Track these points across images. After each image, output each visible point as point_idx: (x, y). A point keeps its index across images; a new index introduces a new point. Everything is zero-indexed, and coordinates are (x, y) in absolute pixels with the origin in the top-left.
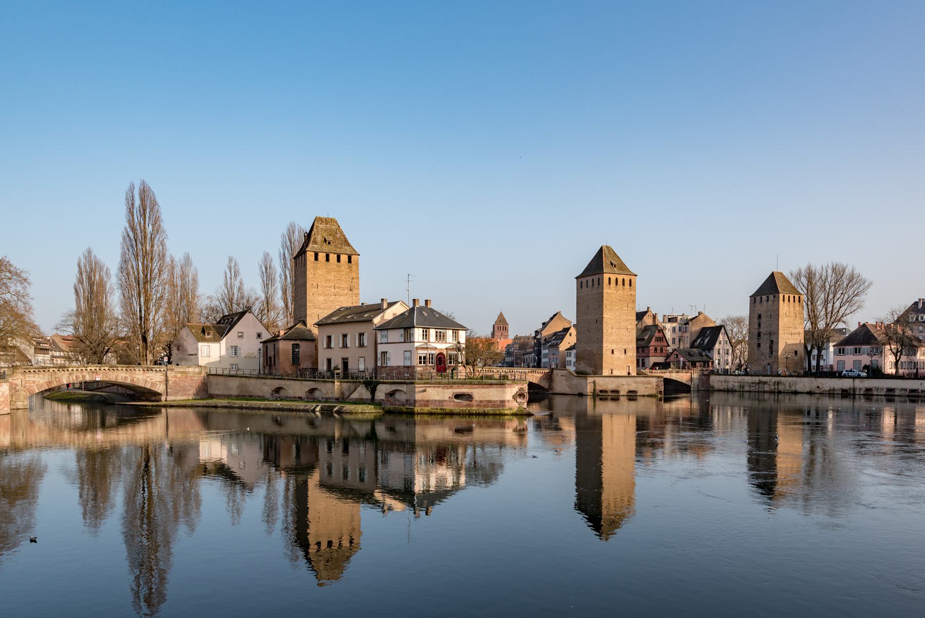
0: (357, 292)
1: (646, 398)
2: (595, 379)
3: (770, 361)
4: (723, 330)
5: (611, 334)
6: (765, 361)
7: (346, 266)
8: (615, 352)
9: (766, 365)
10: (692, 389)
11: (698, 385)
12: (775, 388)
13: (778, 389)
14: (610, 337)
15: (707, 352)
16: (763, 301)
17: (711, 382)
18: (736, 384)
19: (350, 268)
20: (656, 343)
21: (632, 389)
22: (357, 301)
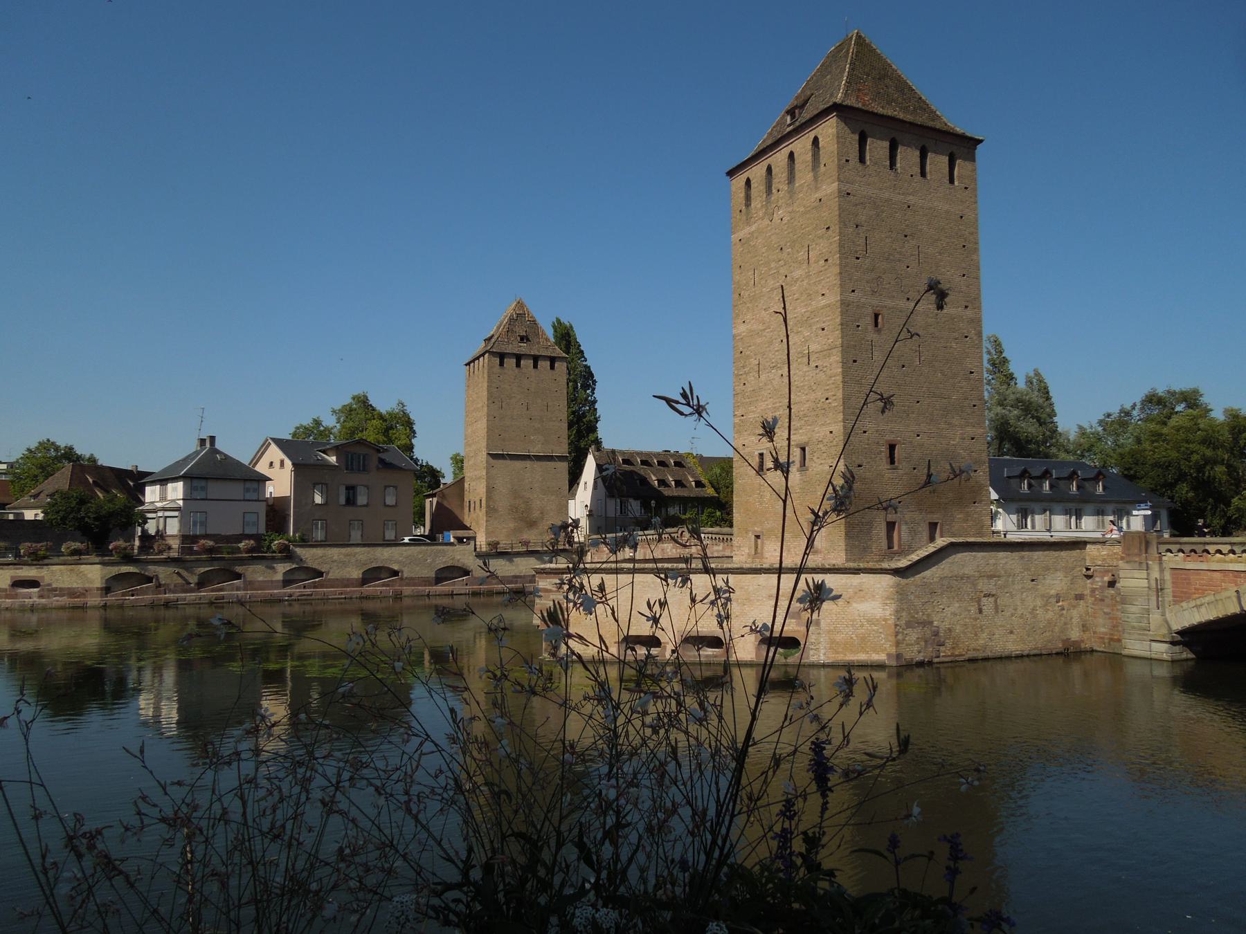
14: (753, 408)
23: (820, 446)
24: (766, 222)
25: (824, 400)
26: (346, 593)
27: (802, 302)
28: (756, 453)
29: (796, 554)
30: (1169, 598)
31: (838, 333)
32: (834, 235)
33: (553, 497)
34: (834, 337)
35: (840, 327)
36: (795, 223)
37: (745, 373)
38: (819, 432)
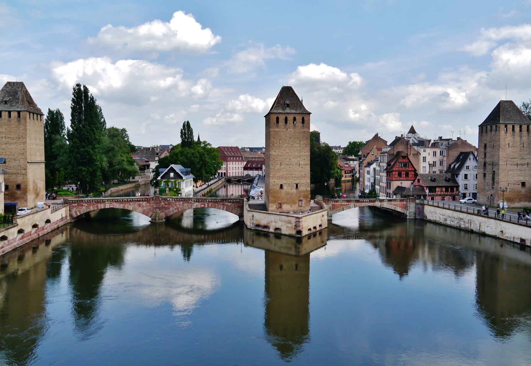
0: (25, 140)
1: (287, 237)
3: (492, 192)
4: (471, 157)
7: (16, 120)
9: (490, 196)
10: (408, 217)
11: (415, 213)
12: (469, 226)
15: (455, 177)
16: (488, 131)
17: (425, 212)
19: (19, 121)
20: (400, 168)
22: (24, 148)
24: (285, 130)
26: (29, 239)
30: (331, 209)
31: (309, 161)
33: (42, 182)
34: (309, 162)
36: (296, 134)
37: (275, 164)
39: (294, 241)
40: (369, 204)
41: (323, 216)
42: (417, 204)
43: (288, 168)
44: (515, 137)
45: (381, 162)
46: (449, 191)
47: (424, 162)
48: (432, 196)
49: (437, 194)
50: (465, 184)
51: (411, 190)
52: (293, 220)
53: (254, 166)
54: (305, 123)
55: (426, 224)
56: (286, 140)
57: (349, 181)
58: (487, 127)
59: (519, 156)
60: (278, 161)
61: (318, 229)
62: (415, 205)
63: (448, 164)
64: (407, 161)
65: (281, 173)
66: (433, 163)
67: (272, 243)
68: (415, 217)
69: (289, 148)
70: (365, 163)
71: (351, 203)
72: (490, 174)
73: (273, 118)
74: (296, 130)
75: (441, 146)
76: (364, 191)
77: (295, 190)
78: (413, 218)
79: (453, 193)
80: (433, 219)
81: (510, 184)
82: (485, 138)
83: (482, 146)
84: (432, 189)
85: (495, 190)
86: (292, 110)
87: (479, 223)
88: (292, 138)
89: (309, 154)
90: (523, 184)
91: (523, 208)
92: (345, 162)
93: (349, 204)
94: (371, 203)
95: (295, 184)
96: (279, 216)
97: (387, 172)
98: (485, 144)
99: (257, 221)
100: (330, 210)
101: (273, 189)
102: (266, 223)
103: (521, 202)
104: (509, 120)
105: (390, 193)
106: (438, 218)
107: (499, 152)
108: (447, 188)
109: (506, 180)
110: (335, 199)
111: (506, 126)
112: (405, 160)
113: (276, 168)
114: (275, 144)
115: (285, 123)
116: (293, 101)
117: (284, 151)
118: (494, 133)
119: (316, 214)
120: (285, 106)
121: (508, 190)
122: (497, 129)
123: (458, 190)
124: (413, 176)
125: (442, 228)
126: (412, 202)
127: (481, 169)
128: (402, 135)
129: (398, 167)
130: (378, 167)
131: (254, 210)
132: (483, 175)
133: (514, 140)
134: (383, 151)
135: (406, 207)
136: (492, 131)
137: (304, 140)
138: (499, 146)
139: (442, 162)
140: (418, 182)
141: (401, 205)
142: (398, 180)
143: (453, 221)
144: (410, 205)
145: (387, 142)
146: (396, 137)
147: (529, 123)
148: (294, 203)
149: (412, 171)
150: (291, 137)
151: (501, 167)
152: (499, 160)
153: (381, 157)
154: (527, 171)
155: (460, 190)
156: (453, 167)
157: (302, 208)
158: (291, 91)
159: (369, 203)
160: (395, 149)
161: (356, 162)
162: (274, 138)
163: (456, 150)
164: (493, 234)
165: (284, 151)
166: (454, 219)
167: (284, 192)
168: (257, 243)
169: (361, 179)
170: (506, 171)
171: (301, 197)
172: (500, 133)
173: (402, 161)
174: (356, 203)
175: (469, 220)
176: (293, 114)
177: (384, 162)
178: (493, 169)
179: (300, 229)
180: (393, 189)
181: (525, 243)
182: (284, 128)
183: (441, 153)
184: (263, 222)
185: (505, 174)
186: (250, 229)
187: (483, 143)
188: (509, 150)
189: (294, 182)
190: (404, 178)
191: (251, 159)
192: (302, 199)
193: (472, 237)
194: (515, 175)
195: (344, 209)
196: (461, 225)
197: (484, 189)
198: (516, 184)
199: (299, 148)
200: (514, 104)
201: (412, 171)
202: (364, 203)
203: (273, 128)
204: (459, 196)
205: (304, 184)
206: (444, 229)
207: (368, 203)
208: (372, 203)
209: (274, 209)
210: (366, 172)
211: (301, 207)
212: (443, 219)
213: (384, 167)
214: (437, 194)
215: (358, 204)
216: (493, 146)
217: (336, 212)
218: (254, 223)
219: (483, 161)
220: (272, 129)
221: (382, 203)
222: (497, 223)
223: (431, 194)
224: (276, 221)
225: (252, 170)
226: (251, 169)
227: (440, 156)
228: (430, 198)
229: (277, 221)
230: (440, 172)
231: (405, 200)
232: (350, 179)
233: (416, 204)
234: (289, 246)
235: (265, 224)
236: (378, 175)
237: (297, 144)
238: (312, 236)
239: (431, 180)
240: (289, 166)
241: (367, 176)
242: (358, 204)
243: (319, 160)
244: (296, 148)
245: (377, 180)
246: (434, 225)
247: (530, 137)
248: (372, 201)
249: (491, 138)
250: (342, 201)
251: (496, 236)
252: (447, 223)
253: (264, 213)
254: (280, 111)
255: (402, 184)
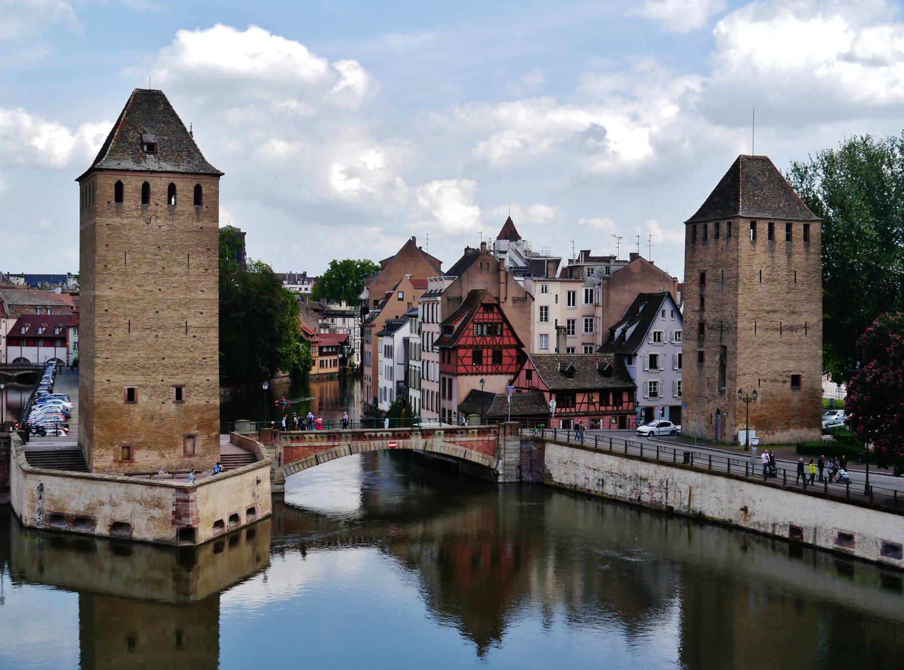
1: (148, 550)
2: (43, 479)
3: (721, 403)
4: (667, 307)
5: (124, 345)
6: (711, 403)
8: (142, 398)
9: (714, 412)
10: (501, 479)
11: (519, 467)
12: (662, 497)
13: (666, 503)
14: (121, 355)
15: (626, 362)
18: (591, 475)
20: (478, 339)
21: (122, 513)
23: (198, 388)
24: (141, 222)
25: (201, 359)
27: (181, 291)
28: (126, 387)
29: (171, 458)
30: (282, 461)
31: (216, 319)
32: (214, 255)
34: (215, 321)
35: (218, 316)
36: (174, 235)
37: (111, 327)
38: (196, 379)
39: (170, 559)
40: (391, 443)
41: (258, 482)
42: (524, 441)
43: (151, 339)
44: (776, 255)
45: (424, 322)
46: (611, 403)
47: (544, 322)
48: (564, 418)
49: (577, 411)
50: (651, 383)
51: (509, 401)
52: (169, 497)
53: (40, 332)
54: (204, 201)
55: (550, 495)
56: (144, 253)
57: (330, 377)
58: (706, 226)
59: (786, 306)
60: (121, 317)
61: (244, 520)
62: (518, 443)
63: (607, 326)
64: (498, 319)
65: (132, 354)
66: (566, 325)
67: (101, 569)
68: (520, 477)
69: (153, 278)
70: (379, 323)
71: (341, 443)
72: (716, 354)
73: (106, 184)
74: (175, 223)
75: (589, 278)
76: (377, 406)
77: (173, 406)
78: (515, 480)
79: (620, 408)
80: (568, 483)
81: (764, 381)
82: (702, 257)
83: (693, 278)
84: (565, 397)
85: (727, 398)
86: (162, 164)
87: (687, 488)
88: (164, 246)
89: (214, 295)
90: (796, 381)
91: (795, 445)
92: (320, 321)
93: (334, 446)
94: (397, 441)
95: (173, 386)
96: (124, 485)
97: (442, 352)
98: (701, 273)
99: (54, 502)
100: (277, 462)
101: (104, 403)
102: (82, 509)
103: (789, 427)
104: (759, 209)
105: (450, 412)
106: (584, 476)
107: (736, 295)
108: (604, 394)
109: (753, 369)
110: (292, 432)
111: (753, 226)
112: (491, 316)
113: (115, 339)
114: (110, 266)
115: (143, 202)
116: (168, 135)
117: (138, 285)
118: (724, 243)
119: (238, 478)
120: (143, 150)
121: (759, 398)
122: (730, 231)
123: (632, 398)
124: (515, 362)
125: (592, 505)
126: (511, 434)
127: (692, 342)
128: (483, 244)
129: (473, 335)
130: (417, 336)
131: (44, 471)
132: (696, 355)
133: (773, 261)
134: (430, 289)
135: (494, 450)
136: (718, 238)
137: (203, 253)
138: (737, 277)
139: (591, 320)
140: (527, 379)
141: (480, 444)
142: (472, 374)
143: (620, 487)
144: (508, 443)
145: (441, 263)
146: (467, 249)
147: (809, 217)
148: (172, 445)
149: (510, 346)
150: (161, 244)
151: (741, 335)
152: (736, 316)
153: (426, 306)
154: (804, 346)
155: (638, 400)
156: (620, 335)
157: (194, 460)
158: (160, 104)
159: (392, 441)
160: (465, 285)
161: (351, 320)
162: (107, 245)
163: (627, 288)
164: (722, 518)
165: (138, 285)
166: (623, 480)
167: (139, 412)
168: (54, 571)
169: (368, 371)
170: (754, 346)
171: (193, 425)
172: (738, 243)
173: (483, 319)
174: (354, 443)
175: (661, 482)
176: (166, 175)
177: (433, 320)
178: (721, 340)
179: (191, 523)
180: (458, 400)
181: (802, 538)
182: (141, 216)
183: (589, 297)
184: (75, 506)
185: (751, 353)
186: (32, 529)
187: (695, 270)
188: (761, 290)
189: (171, 380)
190: (490, 367)
191: (32, 312)
192: (196, 431)
193: (670, 529)
194: (776, 356)
195: (321, 459)
196: (642, 495)
197: (700, 396)
198: (778, 381)
199: (184, 278)
200: (773, 165)
201: (510, 346)
202: (376, 442)
203: (106, 216)
204: (634, 417)
205: (202, 386)
206: (598, 508)
207: (389, 441)
208: (401, 441)
209: (108, 464)
210: (381, 349)
211: (190, 456)
212: (596, 481)
213: (432, 334)
214: (577, 411)
215: (361, 445)
216: (721, 278)
217: (297, 469)
218: (46, 508)
219: (698, 318)
220: (103, 219)
221: (429, 441)
222: (733, 487)
223: (563, 410)
224: (115, 503)
225: (34, 345)
226: (32, 341)
227: (586, 305)
228: (560, 422)
229: (118, 502)
230: (586, 348)
231: (492, 431)
232: (335, 370)
233: (521, 441)
234: (157, 574)
235: (79, 510)
236: (417, 359)
237: (179, 267)
238: (227, 543)
239: (562, 372)
240: (155, 334)
241: (384, 362)
242: (359, 445)
243: (243, 314)
244: (177, 277)
245: (413, 374)
246: (571, 497)
247: (810, 256)
248: (399, 435)
249: (716, 255)
250: (313, 436)
251: (731, 521)
252: (605, 491)
253: (76, 477)
254: (128, 164)
255: (486, 384)
